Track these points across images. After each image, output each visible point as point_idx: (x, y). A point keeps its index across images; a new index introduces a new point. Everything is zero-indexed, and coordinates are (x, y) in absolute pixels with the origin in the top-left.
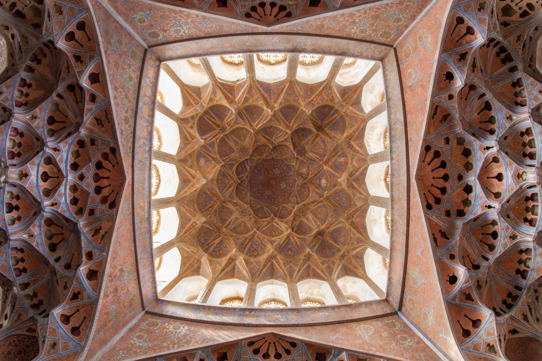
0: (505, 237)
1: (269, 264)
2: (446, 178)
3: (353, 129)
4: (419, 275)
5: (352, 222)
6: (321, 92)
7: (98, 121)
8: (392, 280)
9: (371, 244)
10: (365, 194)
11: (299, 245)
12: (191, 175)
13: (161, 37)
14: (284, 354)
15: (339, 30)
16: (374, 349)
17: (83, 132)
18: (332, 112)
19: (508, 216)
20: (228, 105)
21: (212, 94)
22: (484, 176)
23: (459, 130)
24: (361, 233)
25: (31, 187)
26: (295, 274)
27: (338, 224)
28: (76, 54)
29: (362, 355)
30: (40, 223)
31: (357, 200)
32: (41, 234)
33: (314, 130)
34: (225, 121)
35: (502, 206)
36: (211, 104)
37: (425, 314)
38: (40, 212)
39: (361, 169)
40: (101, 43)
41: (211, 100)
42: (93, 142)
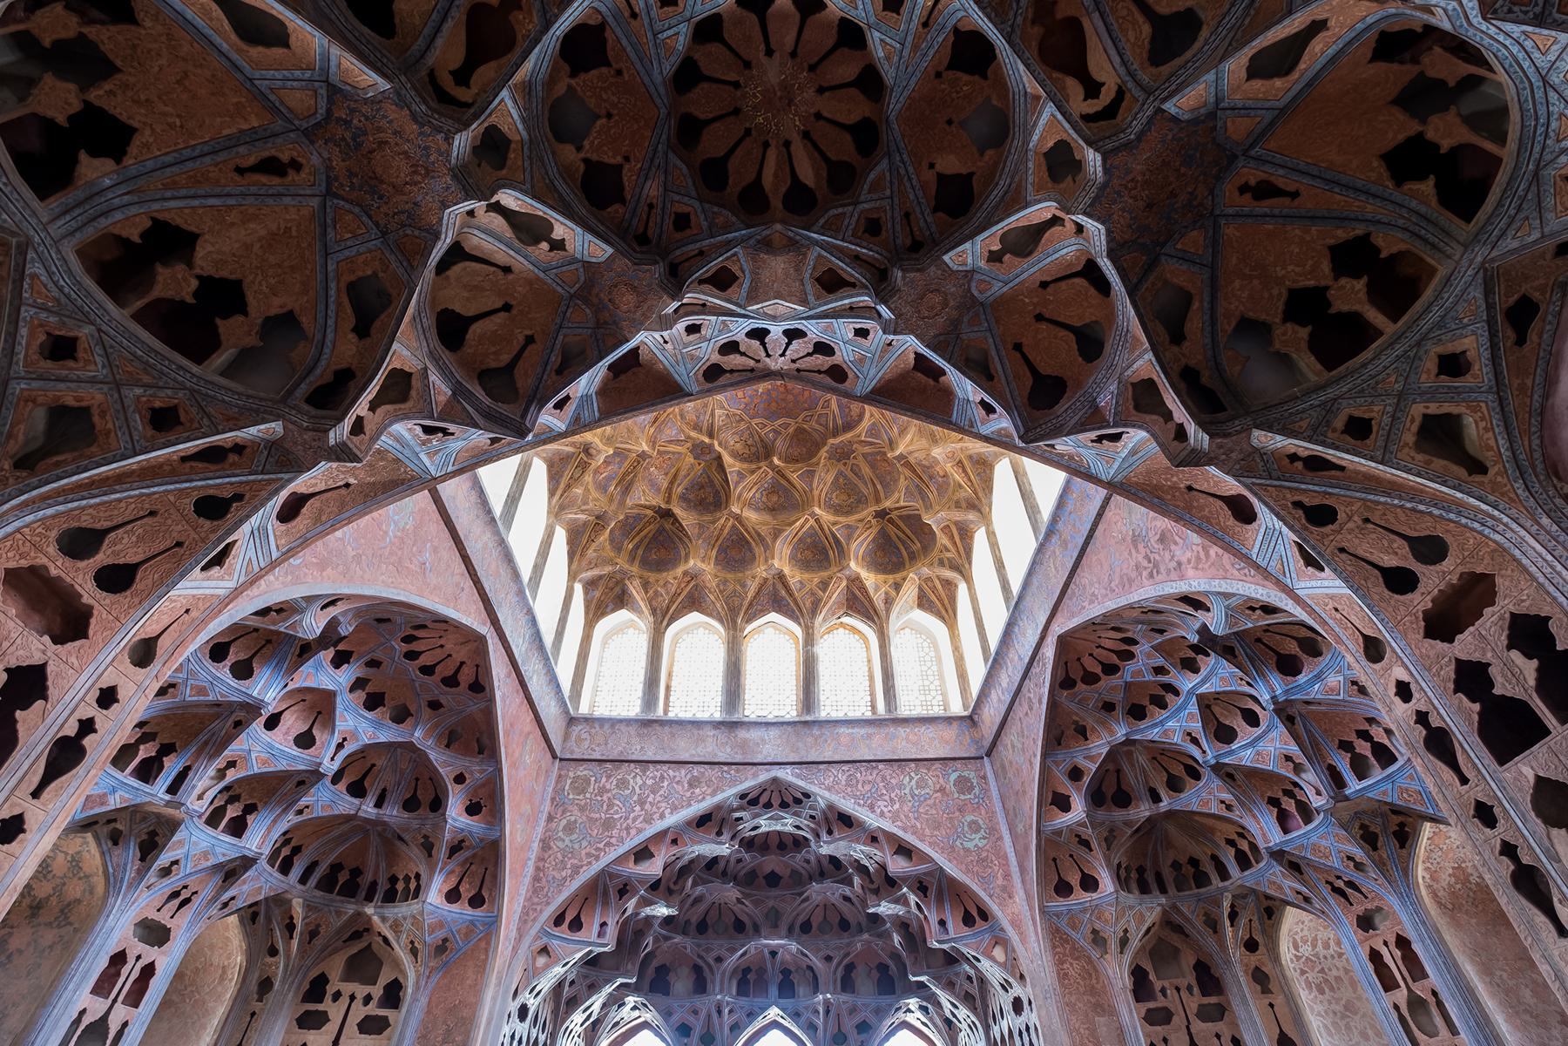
3: (594, 546)
4: (402, 524)
6: (672, 602)
7: (1082, 732)
12: (964, 471)
13: (954, 776)
15: (662, 778)
17: (1121, 732)
18: (640, 552)
20: (864, 574)
21: (893, 600)
30: (1312, 682)
33: (678, 511)
34: (875, 531)
36: (898, 576)
39: (562, 486)
41: (897, 587)
42: (1109, 707)
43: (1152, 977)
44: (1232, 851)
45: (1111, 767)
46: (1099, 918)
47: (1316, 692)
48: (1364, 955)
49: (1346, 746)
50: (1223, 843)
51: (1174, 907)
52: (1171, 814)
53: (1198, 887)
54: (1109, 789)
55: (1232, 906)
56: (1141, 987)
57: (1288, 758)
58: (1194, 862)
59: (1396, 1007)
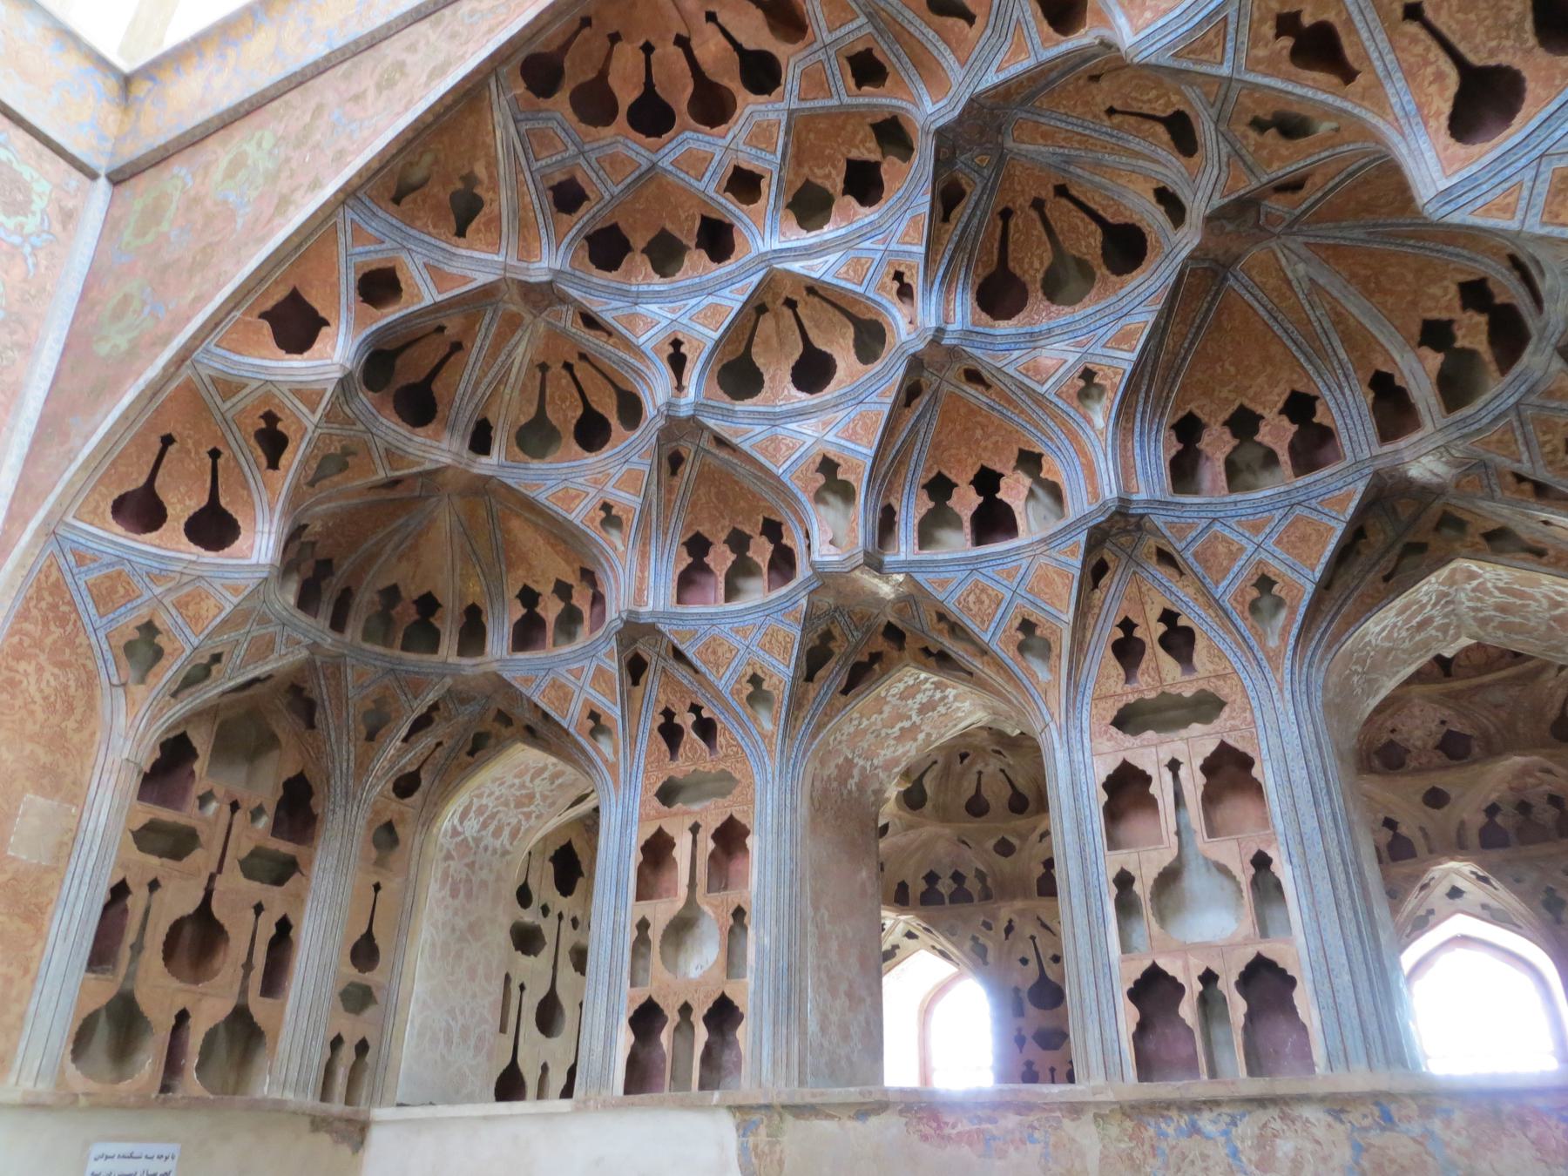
7: (465, 213)
25: (866, 427)
28: (263, 461)
30: (1016, 342)
32: (1068, 330)
38: (953, 353)
40: (142, 383)
43: (199, 766)
44: (519, 611)
45: (453, 327)
46: (180, 605)
47: (1011, 363)
48: (638, 837)
49: (940, 488)
50: (512, 591)
51: (335, 668)
52: (482, 488)
53: (404, 648)
54: (409, 372)
55: (434, 707)
56: (169, 766)
57: (828, 466)
58: (428, 604)
59: (643, 925)
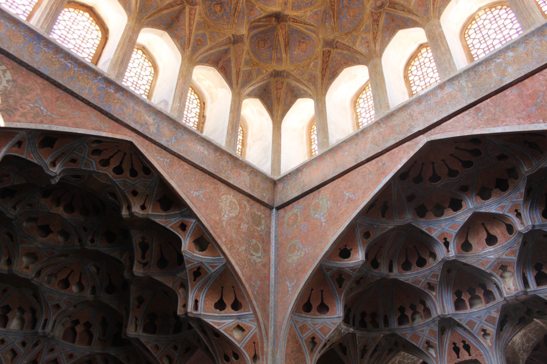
0: (425, 276)
1: (177, 7)
2: (452, 173)
5: (329, 51)
8: (299, 174)
9: (320, 105)
10: (378, 48)
11: (239, 9)
14: (127, 173)
16: (224, 239)
19: (449, 271)
22: (479, 221)
23: (526, 170)
24: (323, 76)
26: (202, 50)
27: (310, 30)
29: (208, 236)
31: (363, 38)
35: (454, 261)
37: (294, 246)
39: (410, 16)
